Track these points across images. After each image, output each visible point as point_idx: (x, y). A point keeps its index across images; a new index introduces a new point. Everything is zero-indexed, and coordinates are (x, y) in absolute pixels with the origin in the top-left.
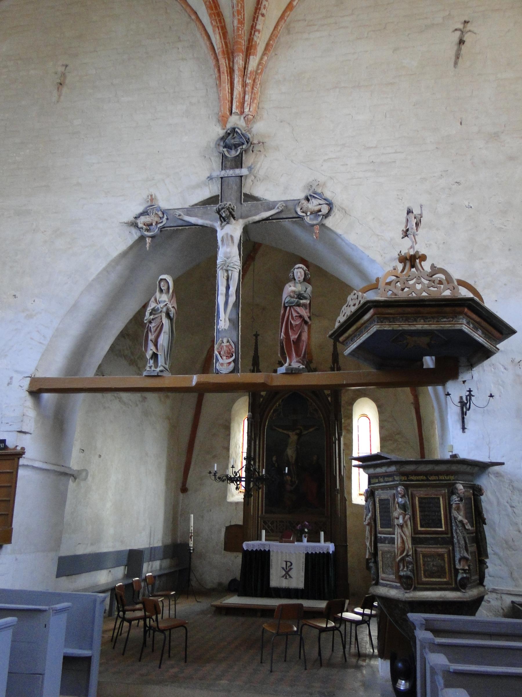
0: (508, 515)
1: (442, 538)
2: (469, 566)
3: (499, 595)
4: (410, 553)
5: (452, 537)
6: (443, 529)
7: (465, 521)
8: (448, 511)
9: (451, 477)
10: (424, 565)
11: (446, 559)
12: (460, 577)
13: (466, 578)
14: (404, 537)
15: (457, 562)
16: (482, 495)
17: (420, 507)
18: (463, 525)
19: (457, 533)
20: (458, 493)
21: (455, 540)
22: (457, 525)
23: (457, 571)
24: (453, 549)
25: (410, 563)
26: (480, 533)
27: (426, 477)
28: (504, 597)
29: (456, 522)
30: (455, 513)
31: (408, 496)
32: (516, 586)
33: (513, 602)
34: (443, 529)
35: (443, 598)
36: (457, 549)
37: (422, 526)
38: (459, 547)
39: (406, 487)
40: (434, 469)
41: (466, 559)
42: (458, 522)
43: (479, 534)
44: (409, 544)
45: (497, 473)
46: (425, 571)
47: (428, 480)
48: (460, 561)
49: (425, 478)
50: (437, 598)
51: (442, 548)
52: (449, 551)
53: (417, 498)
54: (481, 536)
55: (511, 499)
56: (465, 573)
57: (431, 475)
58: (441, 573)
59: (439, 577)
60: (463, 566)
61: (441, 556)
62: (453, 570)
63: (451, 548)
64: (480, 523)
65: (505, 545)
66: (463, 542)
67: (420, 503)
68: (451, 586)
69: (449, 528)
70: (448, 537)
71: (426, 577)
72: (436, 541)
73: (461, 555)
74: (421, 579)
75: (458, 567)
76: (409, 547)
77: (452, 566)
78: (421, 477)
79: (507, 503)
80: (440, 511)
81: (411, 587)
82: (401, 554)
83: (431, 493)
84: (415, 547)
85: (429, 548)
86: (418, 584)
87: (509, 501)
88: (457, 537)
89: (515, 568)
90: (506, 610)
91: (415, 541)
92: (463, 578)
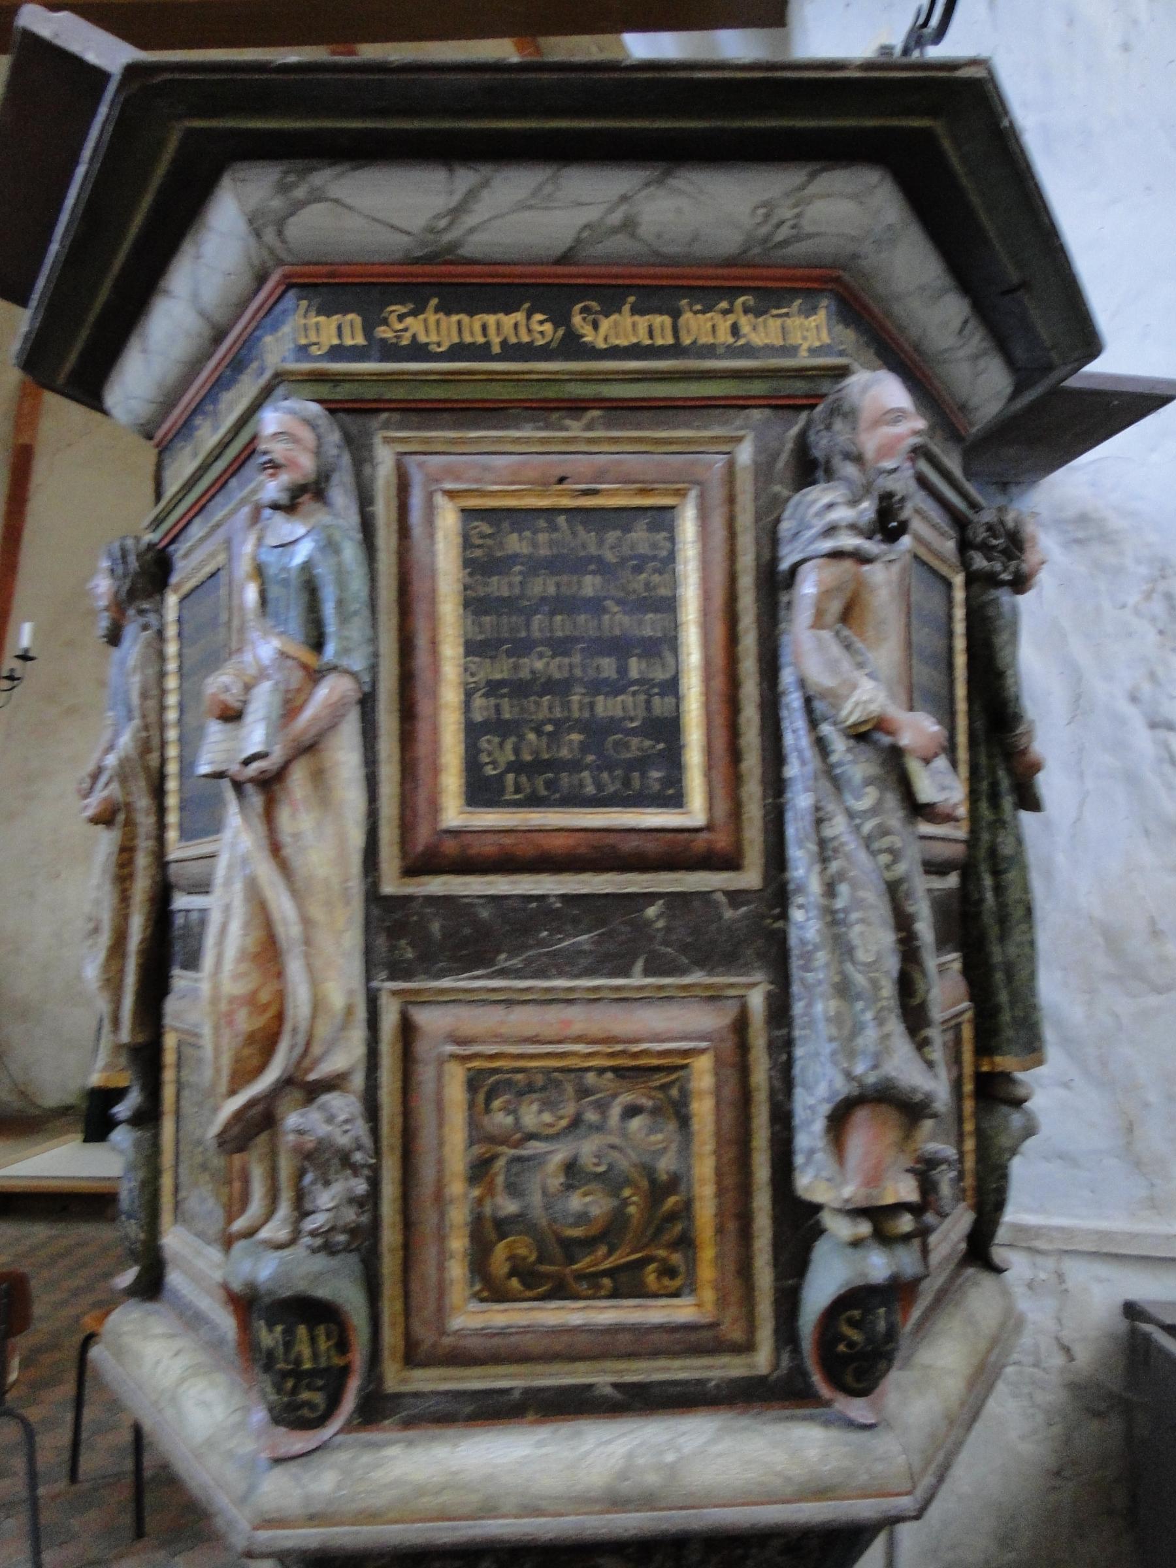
0: (1132, 779)
1: (678, 901)
2: (925, 1171)
3: (1050, 1263)
4: (346, 1056)
5: (778, 893)
6: (695, 810)
7: (918, 729)
8: (749, 642)
9: (795, 322)
10: (479, 1171)
11: (703, 1110)
12: (825, 1282)
13: (898, 1291)
14: (283, 906)
15: (810, 1135)
16: (1020, 583)
17: (475, 604)
18: (895, 766)
19: (825, 851)
20: (857, 459)
21: (805, 924)
22: (833, 778)
23: (799, 1224)
24: (780, 1011)
25: (319, 1159)
26: (996, 873)
27: (560, 319)
28: (1078, 1273)
29: (821, 746)
30: (810, 652)
31: (365, 499)
32: (1153, 1204)
33: (1132, 1310)
34: (695, 810)
35: (648, 1501)
36: (814, 1009)
37: (481, 790)
38: (844, 989)
39: (353, 410)
40: (629, 226)
41: (910, 1110)
42: (840, 746)
43: (988, 881)
44: (331, 973)
45: (1083, 519)
46: (485, 1233)
47: (572, 346)
48: (839, 1118)
49: (542, 330)
50: (583, 1502)
51: (665, 998)
52: (741, 1025)
53: (448, 519)
54: (999, 889)
55: (1152, 676)
56: (884, 1238)
57: (609, 294)
58: (640, 1240)
59: (625, 1283)
60: (874, 1179)
61: (654, 1079)
62: (762, 1201)
63: (757, 1001)
64: (994, 799)
65: (1102, 962)
66: (886, 938)
67: (479, 564)
68: (730, 1368)
69: (754, 811)
70: (735, 897)
71: (493, 1291)
72: (618, 939)
73: (860, 1068)
74: (441, 1312)
75: (812, 1182)
76: (318, 1005)
77: (762, 1172)
78: (505, 325)
79: (1134, 699)
80: (671, 641)
81: (334, 1402)
82: (242, 1076)
83: (597, 461)
84: (410, 1000)
85: (550, 1000)
86: (412, 1357)
87: (1146, 688)
88: (830, 890)
89: (1153, 1097)
90: (1084, 1356)
91: (407, 937)
92: (855, 1300)
